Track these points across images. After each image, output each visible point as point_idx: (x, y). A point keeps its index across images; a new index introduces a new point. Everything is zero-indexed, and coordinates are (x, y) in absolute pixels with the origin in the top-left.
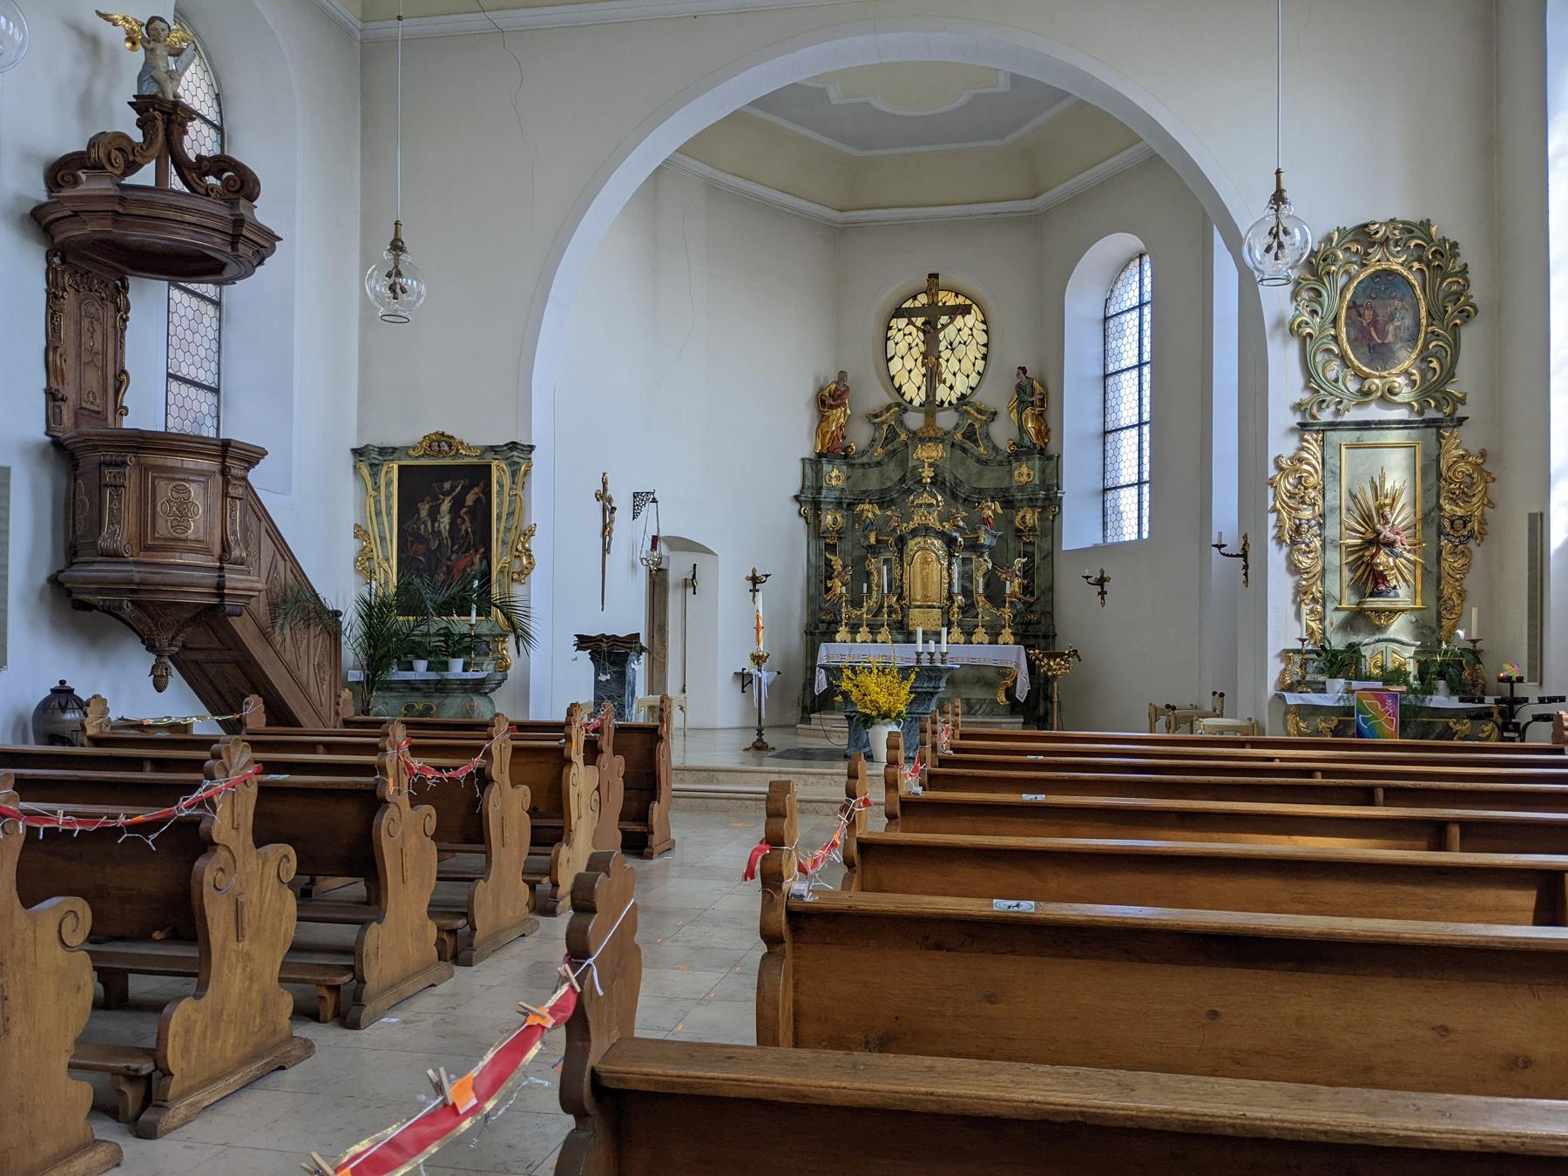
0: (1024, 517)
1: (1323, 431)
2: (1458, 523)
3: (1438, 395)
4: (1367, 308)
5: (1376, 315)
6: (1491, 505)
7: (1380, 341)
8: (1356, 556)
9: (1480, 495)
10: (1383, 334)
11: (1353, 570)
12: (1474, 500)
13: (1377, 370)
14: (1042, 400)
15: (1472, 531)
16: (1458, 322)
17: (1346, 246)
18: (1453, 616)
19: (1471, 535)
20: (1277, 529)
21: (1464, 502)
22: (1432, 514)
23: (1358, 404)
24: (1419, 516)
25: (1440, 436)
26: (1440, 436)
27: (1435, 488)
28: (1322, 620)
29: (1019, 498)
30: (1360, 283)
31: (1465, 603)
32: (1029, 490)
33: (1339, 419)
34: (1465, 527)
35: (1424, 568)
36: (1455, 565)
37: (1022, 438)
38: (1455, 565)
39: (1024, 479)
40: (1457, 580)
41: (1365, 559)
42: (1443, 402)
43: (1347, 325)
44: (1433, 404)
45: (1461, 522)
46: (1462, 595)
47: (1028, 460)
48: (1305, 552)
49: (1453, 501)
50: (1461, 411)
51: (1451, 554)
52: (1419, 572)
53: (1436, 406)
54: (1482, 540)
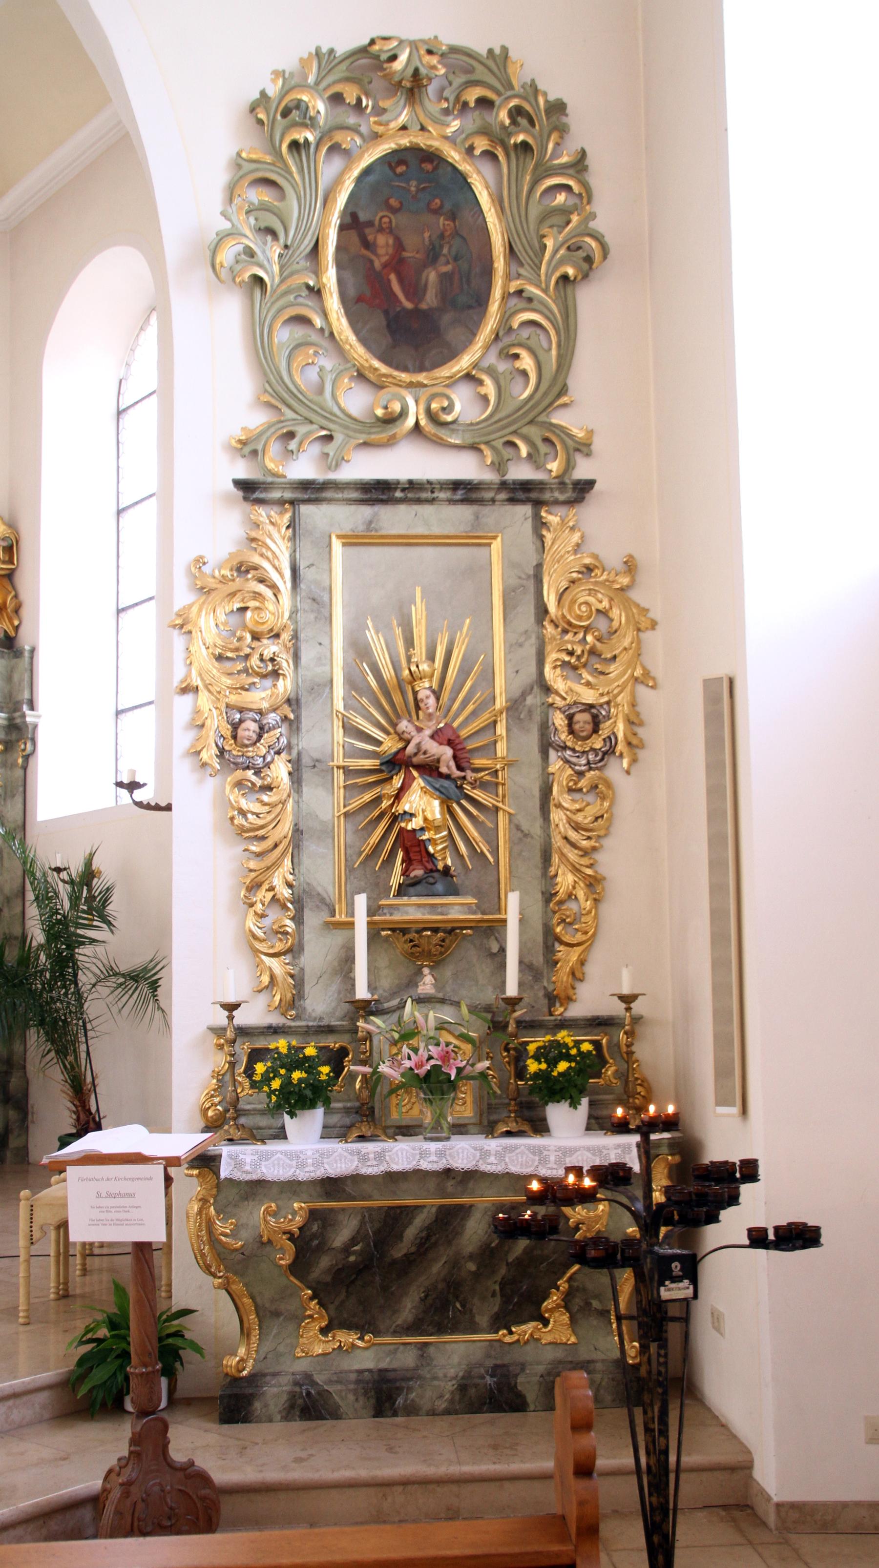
1: (292, 502)
2: (582, 718)
3: (534, 432)
4: (381, 230)
5: (399, 246)
6: (647, 679)
7: (409, 305)
8: (367, 797)
10: (414, 291)
12: (614, 669)
13: (405, 369)
16: (571, 272)
17: (338, 88)
18: (579, 937)
19: (609, 751)
20: (192, 735)
22: (530, 700)
23: (366, 444)
25: (539, 524)
26: (539, 524)
27: (533, 640)
28: (294, 951)
30: (367, 172)
31: (604, 907)
33: (332, 476)
34: (596, 730)
40: (585, 853)
41: (385, 804)
42: (543, 448)
43: (340, 265)
44: (524, 450)
45: (586, 717)
46: (594, 883)
49: (570, 668)
50: (583, 470)
51: (570, 790)
53: (530, 456)
54: (634, 761)
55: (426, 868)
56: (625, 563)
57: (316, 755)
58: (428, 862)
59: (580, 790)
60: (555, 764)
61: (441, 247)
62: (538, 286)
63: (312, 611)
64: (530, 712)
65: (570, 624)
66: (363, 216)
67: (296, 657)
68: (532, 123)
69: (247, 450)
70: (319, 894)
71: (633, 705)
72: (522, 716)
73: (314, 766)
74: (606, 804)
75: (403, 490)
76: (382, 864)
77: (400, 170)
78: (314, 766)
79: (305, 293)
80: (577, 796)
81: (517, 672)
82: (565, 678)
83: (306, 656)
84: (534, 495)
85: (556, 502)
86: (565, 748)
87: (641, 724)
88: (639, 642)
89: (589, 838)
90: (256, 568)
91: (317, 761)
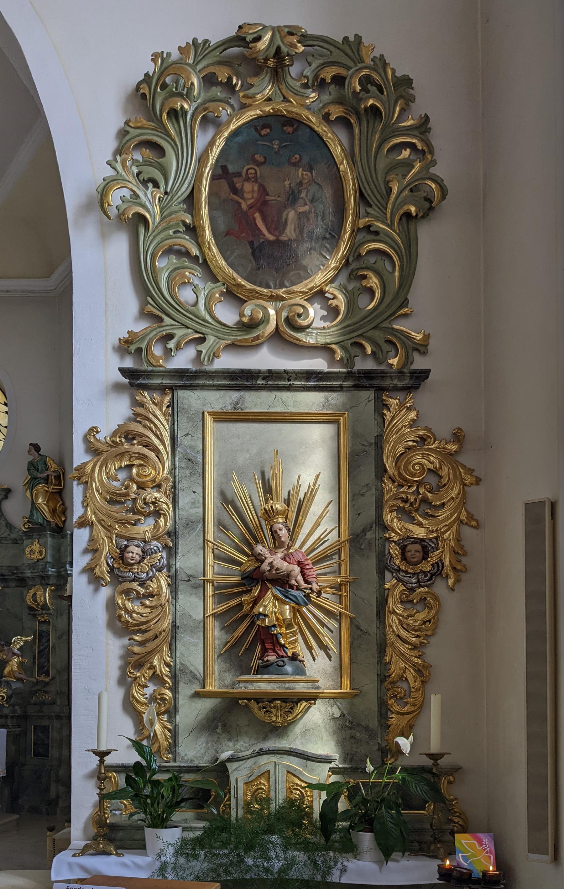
0: (35, 594)
2: (414, 550)
3: (378, 335)
5: (263, 191)
8: (233, 603)
9: (452, 505)
11: (228, 628)
12: (443, 514)
14: (58, 478)
15: (439, 567)
21: (426, 516)
22: (369, 535)
24: (345, 536)
27: (373, 491)
29: (29, 575)
32: (40, 567)
35: (355, 626)
36: (411, 621)
37: (32, 514)
38: (411, 621)
39: (36, 556)
41: (246, 608)
42: (386, 347)
44: (369, 350)
47: (40, 536)
48: (140, 597)
52: (345, 635)
53: (373, 353)
55: (278, 654)
56: (454, 434)
57: (190, 572)
58: (280, 650)
59: (412, 601)
60: (390, 582)
61: (300, 192)
62: (383, 223)
63: (188, 468)
64: (369, 544)
65: (405, 480)
66: (231, 168)
67: (175, 502)
68: (381, 91)
69: (133, 348)
70: (191, 672)
71: (458, 540)
72: (362, 547)
73: (189, 580)
74: (433, 612)
75: (264, 379)
76: (244, 651)
77: (263, 132)
78: (189, 580)
79: (182, 229)
80: (409, 606)
81: (359, 514)
82: (399, 519)
83: (184, 500)
84: (375, 382)
85: (396, 389)
86: (399, 570)
87: (465, 554)
88: (465, 493)
89: (418, 636)
90: (141, 435)
91: (191, 576)
